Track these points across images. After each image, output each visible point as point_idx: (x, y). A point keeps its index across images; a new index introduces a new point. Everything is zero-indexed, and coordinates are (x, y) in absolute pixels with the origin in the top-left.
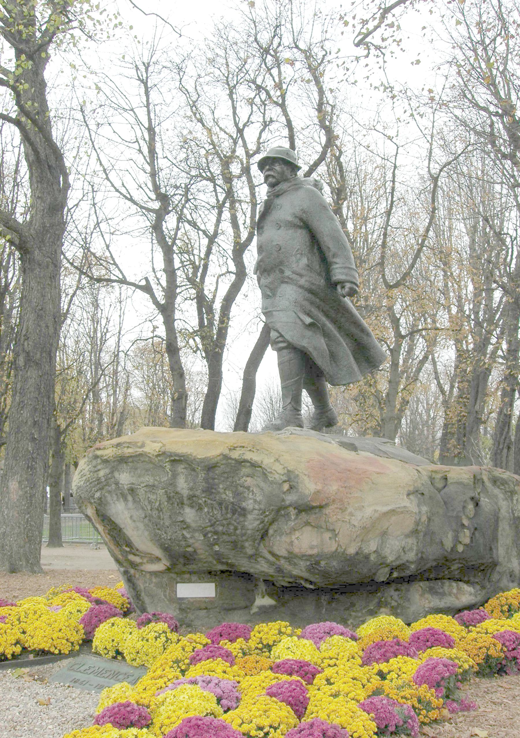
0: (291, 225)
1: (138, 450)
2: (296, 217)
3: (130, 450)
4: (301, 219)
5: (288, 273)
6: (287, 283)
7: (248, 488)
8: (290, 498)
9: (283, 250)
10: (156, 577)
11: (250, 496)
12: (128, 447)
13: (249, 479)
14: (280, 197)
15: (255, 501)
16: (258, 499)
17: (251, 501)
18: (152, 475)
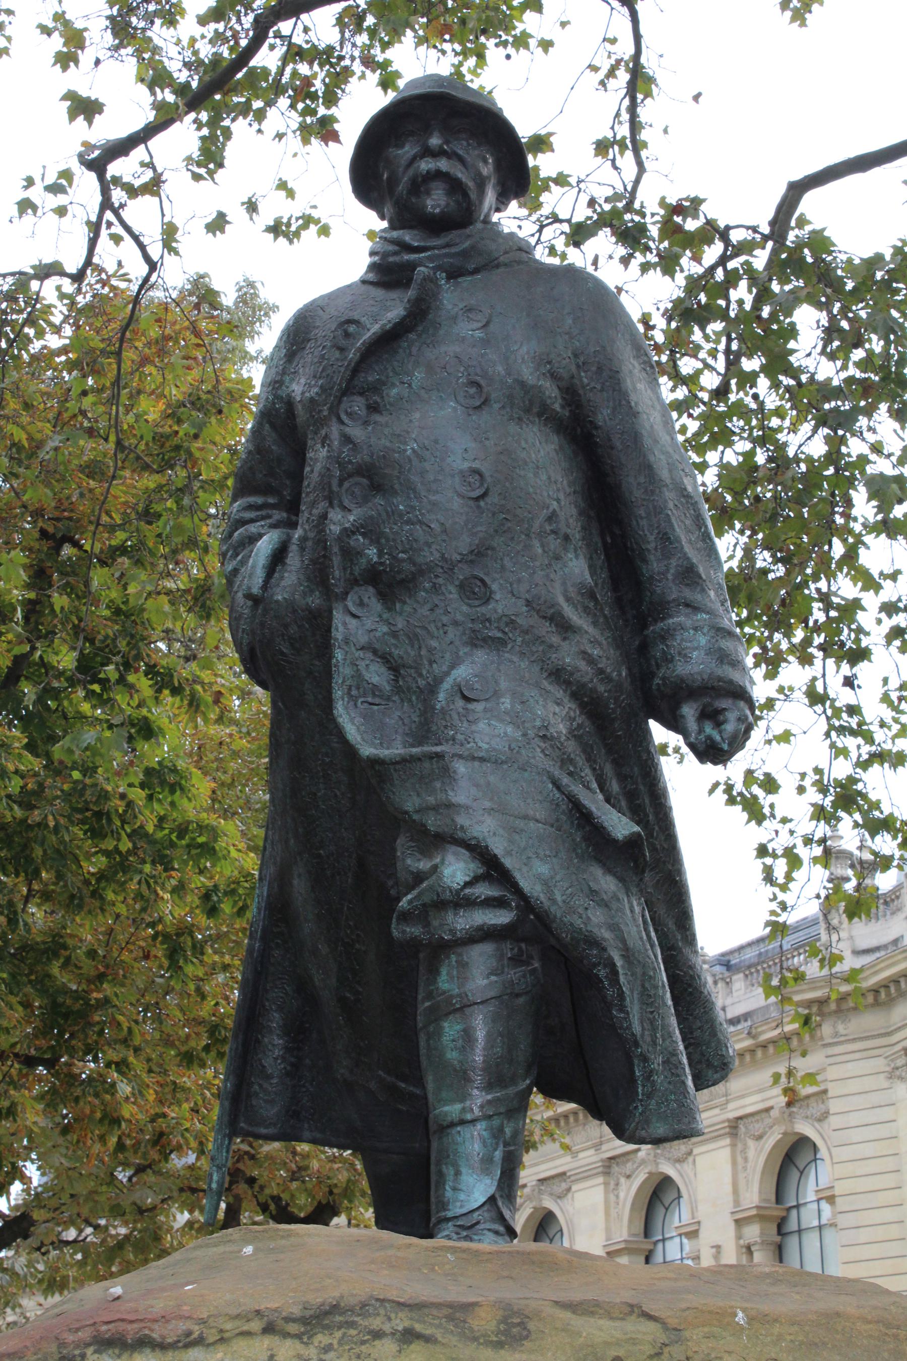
0: (529, 406)
4: (571, 394)
5: (503, 603)
6: (498, 644)
14: (466, 281)
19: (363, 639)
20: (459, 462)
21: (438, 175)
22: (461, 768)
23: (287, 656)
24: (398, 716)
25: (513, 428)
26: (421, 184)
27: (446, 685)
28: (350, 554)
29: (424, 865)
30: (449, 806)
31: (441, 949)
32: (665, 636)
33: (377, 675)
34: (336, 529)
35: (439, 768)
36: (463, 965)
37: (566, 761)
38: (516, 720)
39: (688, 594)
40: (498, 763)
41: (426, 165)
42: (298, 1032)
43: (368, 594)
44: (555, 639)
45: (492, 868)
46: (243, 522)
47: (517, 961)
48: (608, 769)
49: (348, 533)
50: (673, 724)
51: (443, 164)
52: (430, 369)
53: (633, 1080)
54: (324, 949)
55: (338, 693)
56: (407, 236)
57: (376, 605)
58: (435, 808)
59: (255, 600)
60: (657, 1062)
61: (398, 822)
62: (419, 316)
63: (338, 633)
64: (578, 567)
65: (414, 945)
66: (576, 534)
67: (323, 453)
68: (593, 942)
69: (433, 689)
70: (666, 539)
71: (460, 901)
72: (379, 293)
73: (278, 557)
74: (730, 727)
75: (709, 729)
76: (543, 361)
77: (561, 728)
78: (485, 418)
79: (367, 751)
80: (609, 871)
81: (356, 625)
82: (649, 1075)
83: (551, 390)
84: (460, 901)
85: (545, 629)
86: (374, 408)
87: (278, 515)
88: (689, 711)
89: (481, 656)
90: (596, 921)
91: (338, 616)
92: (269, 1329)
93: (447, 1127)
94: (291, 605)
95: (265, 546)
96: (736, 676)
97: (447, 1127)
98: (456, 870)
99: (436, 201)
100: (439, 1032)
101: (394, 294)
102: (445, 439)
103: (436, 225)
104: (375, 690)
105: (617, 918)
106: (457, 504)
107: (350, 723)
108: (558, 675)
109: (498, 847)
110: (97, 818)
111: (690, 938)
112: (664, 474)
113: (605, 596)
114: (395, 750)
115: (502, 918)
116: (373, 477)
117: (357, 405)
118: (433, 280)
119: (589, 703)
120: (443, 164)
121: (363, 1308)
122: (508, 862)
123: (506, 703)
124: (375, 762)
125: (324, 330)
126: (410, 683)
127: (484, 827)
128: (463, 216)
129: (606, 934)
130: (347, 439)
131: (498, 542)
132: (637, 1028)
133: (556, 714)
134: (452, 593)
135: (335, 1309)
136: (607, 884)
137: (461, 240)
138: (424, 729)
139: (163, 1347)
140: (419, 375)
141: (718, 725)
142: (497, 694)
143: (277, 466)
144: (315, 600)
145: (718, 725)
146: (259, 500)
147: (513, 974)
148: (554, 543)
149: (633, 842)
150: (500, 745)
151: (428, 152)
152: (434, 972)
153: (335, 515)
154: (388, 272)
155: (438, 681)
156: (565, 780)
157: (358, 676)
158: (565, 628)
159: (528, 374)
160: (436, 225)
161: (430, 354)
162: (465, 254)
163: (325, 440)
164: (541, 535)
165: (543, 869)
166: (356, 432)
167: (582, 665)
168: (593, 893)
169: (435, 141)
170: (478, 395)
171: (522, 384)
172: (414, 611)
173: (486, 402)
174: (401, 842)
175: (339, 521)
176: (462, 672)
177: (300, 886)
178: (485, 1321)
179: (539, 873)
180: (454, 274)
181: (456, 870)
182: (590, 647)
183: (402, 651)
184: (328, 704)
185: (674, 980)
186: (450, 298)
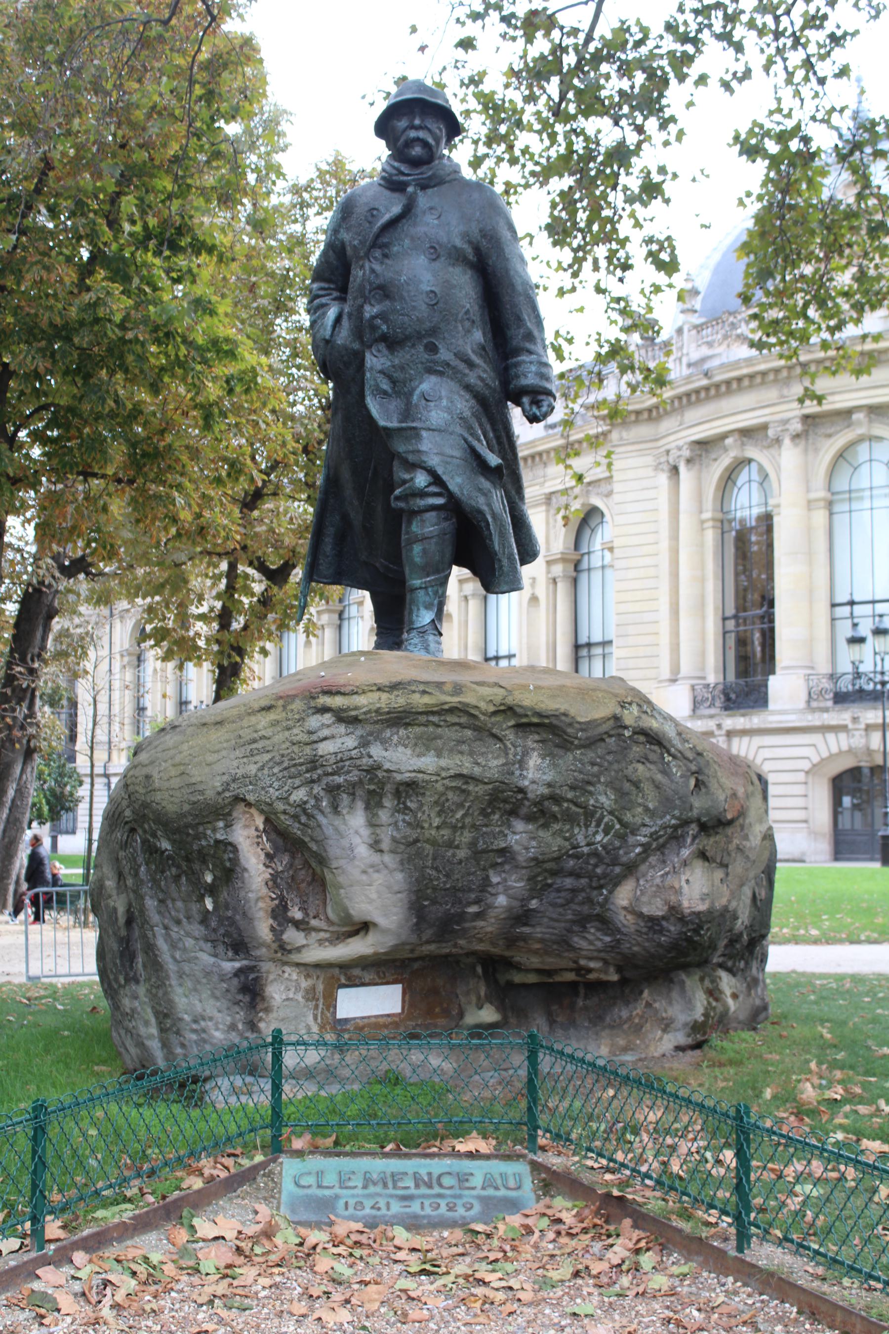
0: (457, 257)
1: (448, 699)
2: (470, 242)
3: (426, 699)
4: (477, 250)
5: (444, 354)
6: (441, 374)
7: (636, 784)
8: (698, 803)
9: (441, 305)
10: (308, 976)
11: (640, 801)
12: (424, 692)
13: (640, 767)
14: (430, 191)
15: (647, 809)
16: (651, 806)
17: (640, 810)
18: (471, 753)
19: (379, 367)
20: (425, 287)
21: (418, 139)
22: (424, 434)
23: (338, 365)
24: (395, 405)
25: (451, 269)
26: (410, 143)
27: (417, 392)
28: (374, 328)
29: (407, 476)
30: (419, 451)
31: (414, 513)
32: (517, 365)
33: (385, 386)
34: (367, 315)
35: (415, 433)
36: (423, 521)
37: (470, 428)
38: (448, 410)
39: (528, 345)
40: (439, 431)
41: (413, 134)
42: (341, 538)
43: (382, 346)
44: (467, 371)
45: (437, 480)
46: (318, 297)
47: (446, 519)
48: (488, 427)
49: (373, 318)
50: (518, 403)
51: (421, 134)
52: (412, 239)
53: (494, 569)
54: (356, 503)
55: (367, 392)
56: (403, 168)
57: (385, 351)
58: (413, 452)
59: (327, 342)
60: (505, 562)
61: (393, 455)
62: (407, 211)
63: (368, 364)
64: (478, 336)
65: (402, 510)
66: (477, 318)
67: (361, 273)
68: (480, 512)
69: (411, 393)
70: (519, 319)
71: (422, 494)
72: (387, 193)
73: (338, 320)
74: (544, 409)
75: (535, 409)
76: (465, 236)
77: (467, 413)
78: (437, 265)
79: (382, 423)
80: (487, 479)
81: (376, 361)
82: (501, 567)
83: (469, 251)
84: (422, 494)
85: (462, 366)
86: (386, 256)
87: (335, 294)
88: (526, 400)
89: (433, 379)
90: (481, 502)
91: (368, 356)
92: (379, 689)
93: (413, 590)
94: (346, 348)
95: (332, 313)
96: (548, 385)
97: (413, 590)
98: (421, 480)
99: (417, 151)
100: (412, 550)
101: (396, 195)
102: (421, 273)
103: (416, 163)
104: (385, 393)
105: (492, 502)
106: (424, 307)
107: (374, 406)
108: (468, 388)
109: (440, 471)
110: (164, 333)
111: (522, 498)
112: (520, 288)
113: (490, 348)
114: (394, 424)
115: (440, 501)
116: (384, 291)
117: (378, 253)
118: (415, 193)
119: (481, 400)
120: (421, 134)
121: (409, 683)
122: (444, 478)
123: (444, 402)
124: (386, 429)
125: (360, 210)
126: (399, 387)
127: (434, 461)
128: (430, 156)
129: (485, 508)
130: (373, 271)
131: (442, 325)
132: (497, 548)
133: (464, 405)
134: (421, 348)
135: (400, 683)
136: (486, 484)
137: (427, 172)
138: (407, 413)
139: (344, 694)
140: (407, 242)
141: (539, 407)
142: (440, 398)
143: (335, 272)
144: (356, 346)
145: (539, 407)
146: (326, 285)
147: (446, 524)
148: (467, 324)
149: (499, 468)
150: (441, 423)
151: (413, 127)
152: (410, 523)
153: (367, 308)
154: (392, 183)
155: (414, 390)
156: (470, 439)
157: (377, 385)
158: (471, 365)
159: (458, 242)
160: (416, 163)
161: (413, 231)
162: (430, 178)
163: (362, 267)
164: (462, 321)
165: (459, 480)
166: (377, 267)
167: (479, 383)
168: (480, 490)
169: (417, 122)
170: (435, 252)
171: (455, 247)
172: (402, 356)
173: (438, 257)
174: (396, 463)
175: (370, 311)
176: (425, 386)
177: (346, 474)
178: (448, 688)
179: (456, 482)
180: (424, 187)
181: (421, 480)
182: (483, 374)
183: (397, 375)
184: (362, 397)
185: (513, 517)
186: (423, 200)
